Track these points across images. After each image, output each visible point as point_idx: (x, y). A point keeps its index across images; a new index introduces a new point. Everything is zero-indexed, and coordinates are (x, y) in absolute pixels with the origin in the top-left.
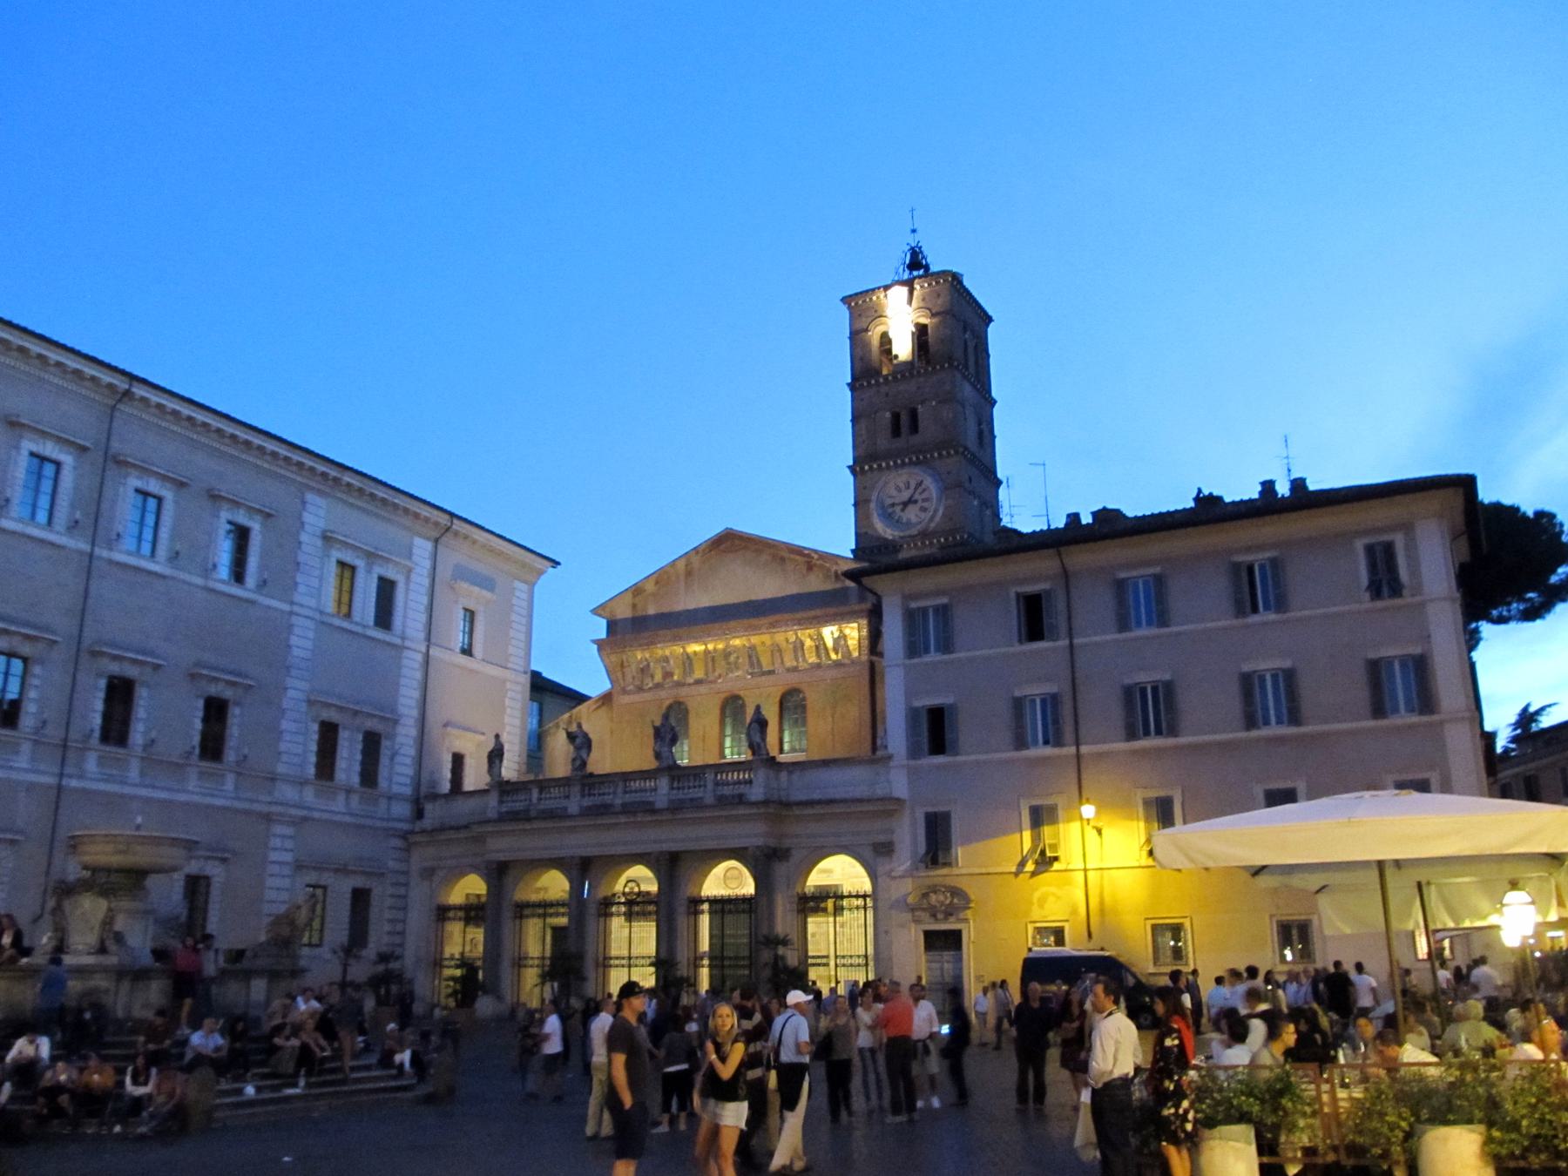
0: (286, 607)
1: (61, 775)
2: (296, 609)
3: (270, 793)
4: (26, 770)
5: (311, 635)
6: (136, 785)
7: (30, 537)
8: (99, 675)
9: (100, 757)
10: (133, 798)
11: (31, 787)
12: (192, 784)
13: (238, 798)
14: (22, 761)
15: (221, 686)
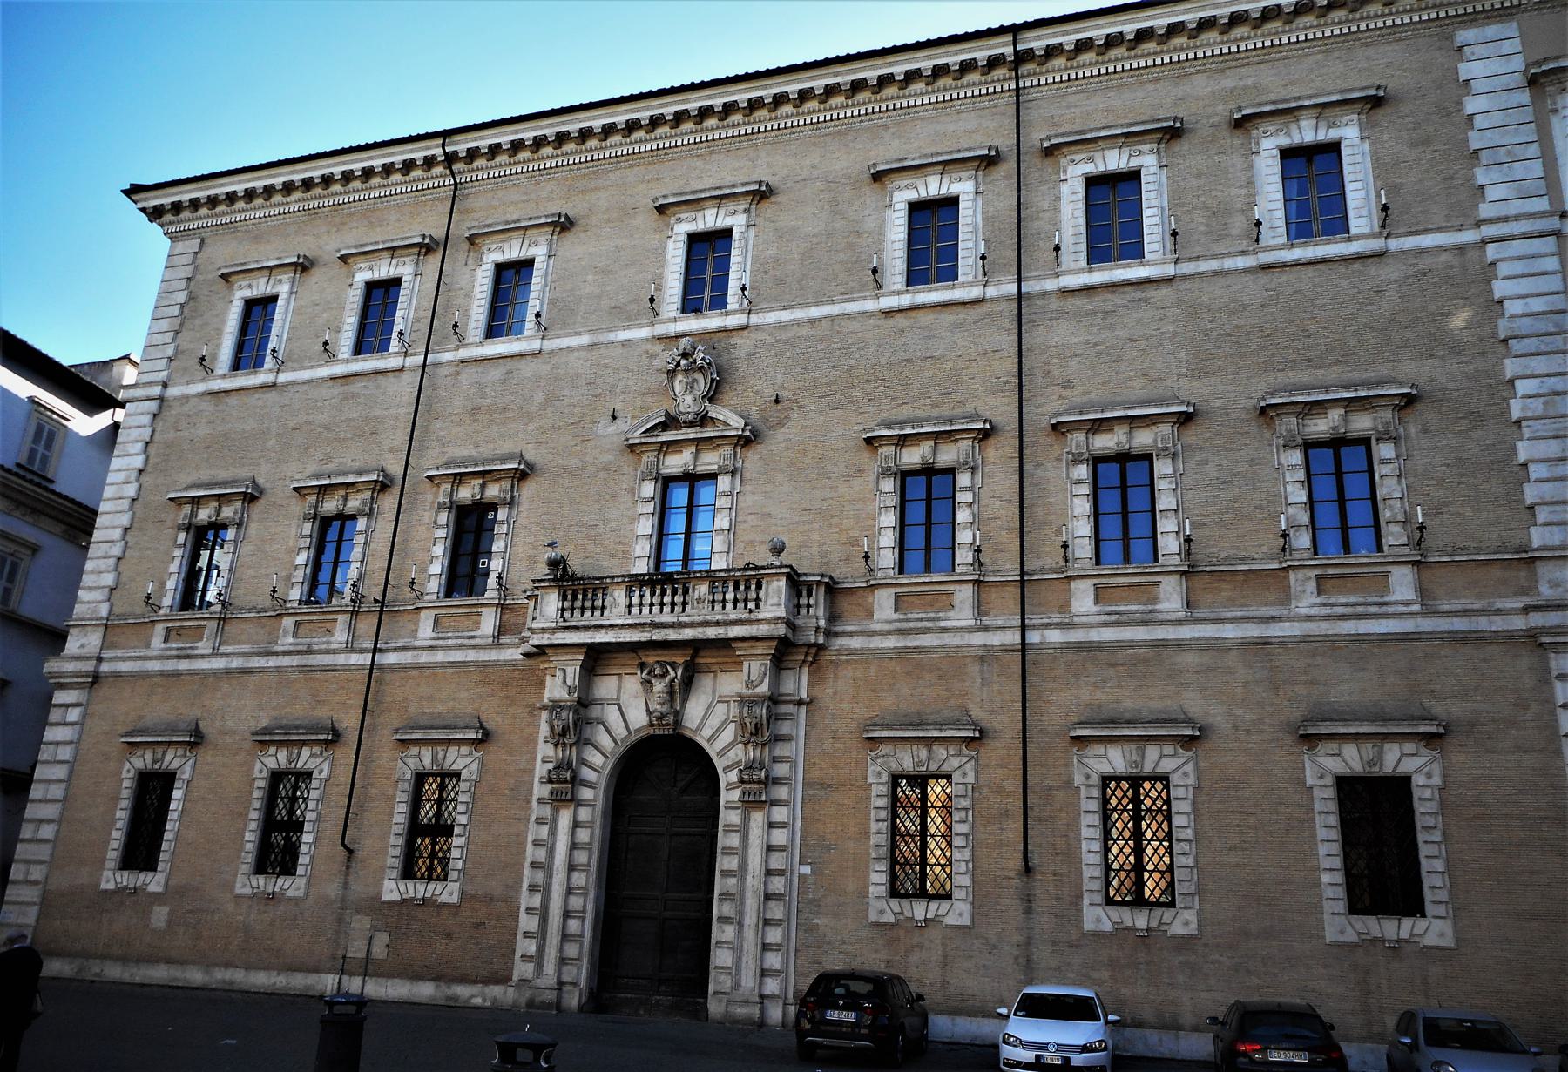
0: (1469, 236)
1: (1023, 628)
2: (1488, 231)
3: (1524, 592)
4: (968, 630)
5: (1552, 263)
6: (1179, 622)
7: (924, 307)
8: (1076, 460)
9: (1097, 588)
10: (1180, 645)
11: (986, 656)
12: (1306, 600)
13: (1429, 612)
14: (962, 616)
15: (1335, 415)
